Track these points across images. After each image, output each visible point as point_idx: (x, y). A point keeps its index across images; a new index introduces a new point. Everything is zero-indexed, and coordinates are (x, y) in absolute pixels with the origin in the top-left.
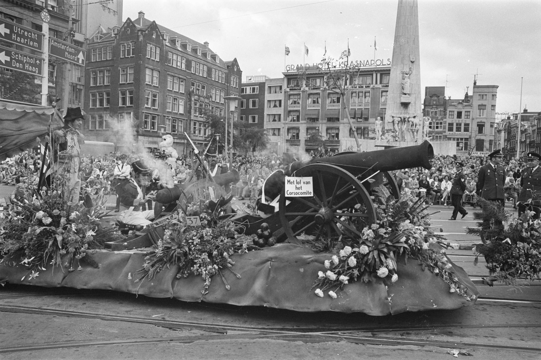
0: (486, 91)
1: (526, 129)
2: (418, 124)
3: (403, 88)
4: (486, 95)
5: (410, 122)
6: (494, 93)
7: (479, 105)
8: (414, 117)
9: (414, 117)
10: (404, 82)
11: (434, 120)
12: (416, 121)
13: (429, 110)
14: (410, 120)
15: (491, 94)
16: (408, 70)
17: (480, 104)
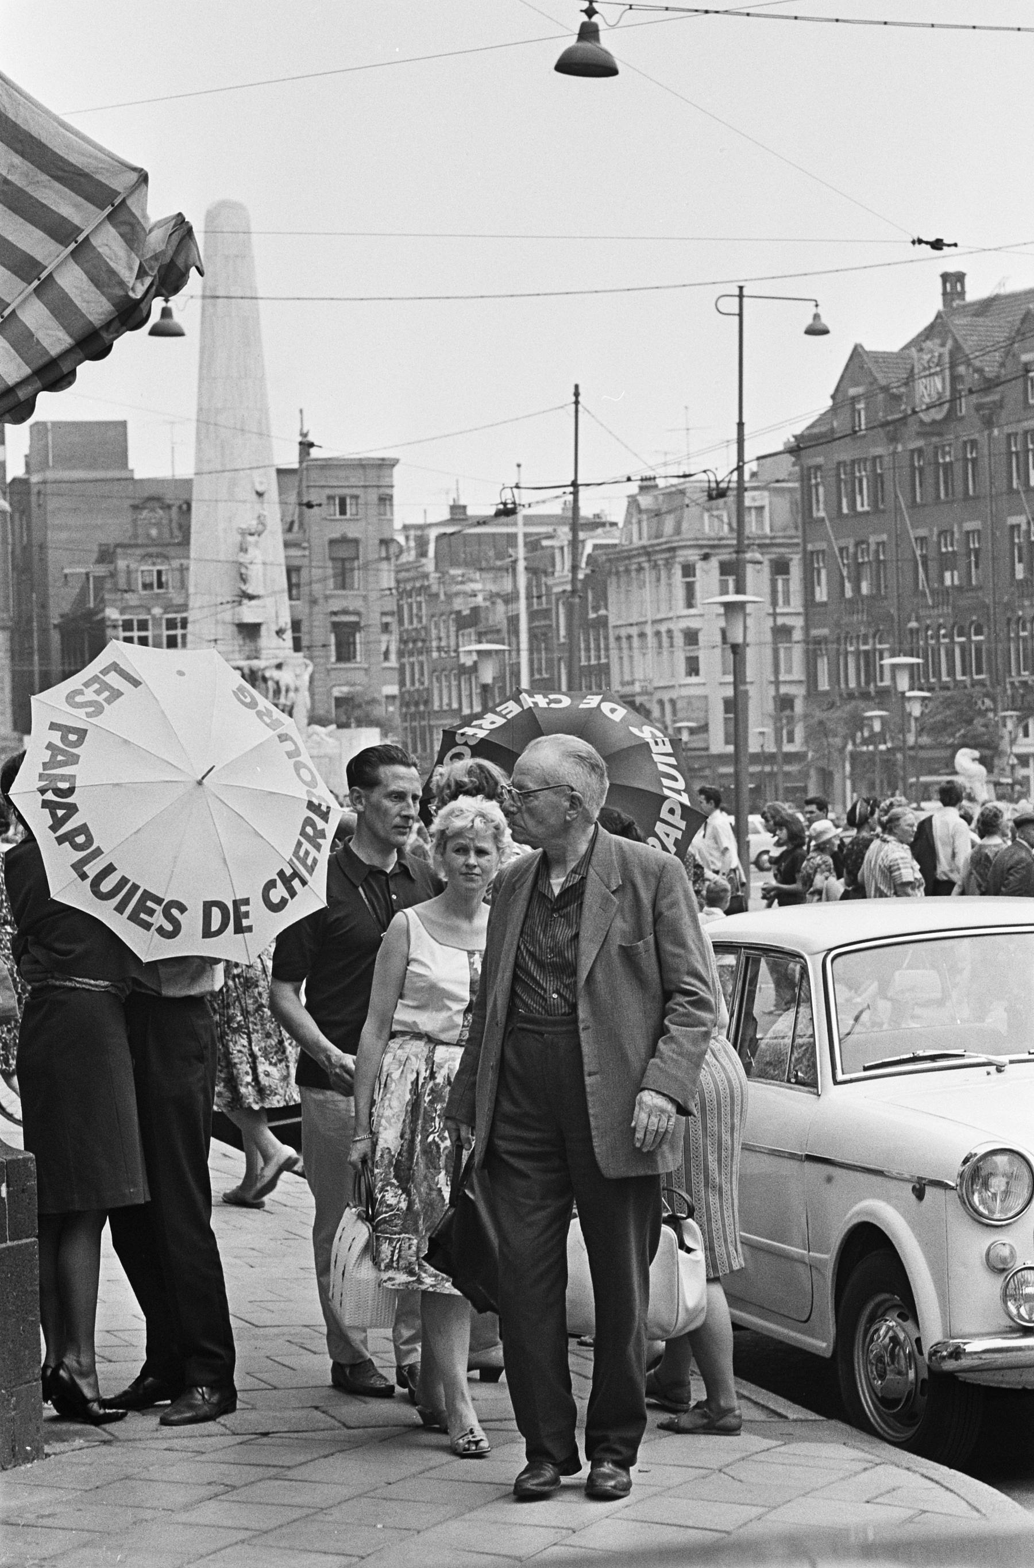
0: (353, 481)
1: (475, 610)
2: (292, 687)
3: (244, 579)
4: (356, 497)
5: (270, 683)
6: (382, 491)
7: (332, 542)
8: (279, 666)
9: (279, 666)
10: (243, 558)
11: (157, 611)
12: (285, 677)
13: (133, 566)
14: (267, 674)
15: (373, 496)
16: (255, 522)
17: (336, 535)
